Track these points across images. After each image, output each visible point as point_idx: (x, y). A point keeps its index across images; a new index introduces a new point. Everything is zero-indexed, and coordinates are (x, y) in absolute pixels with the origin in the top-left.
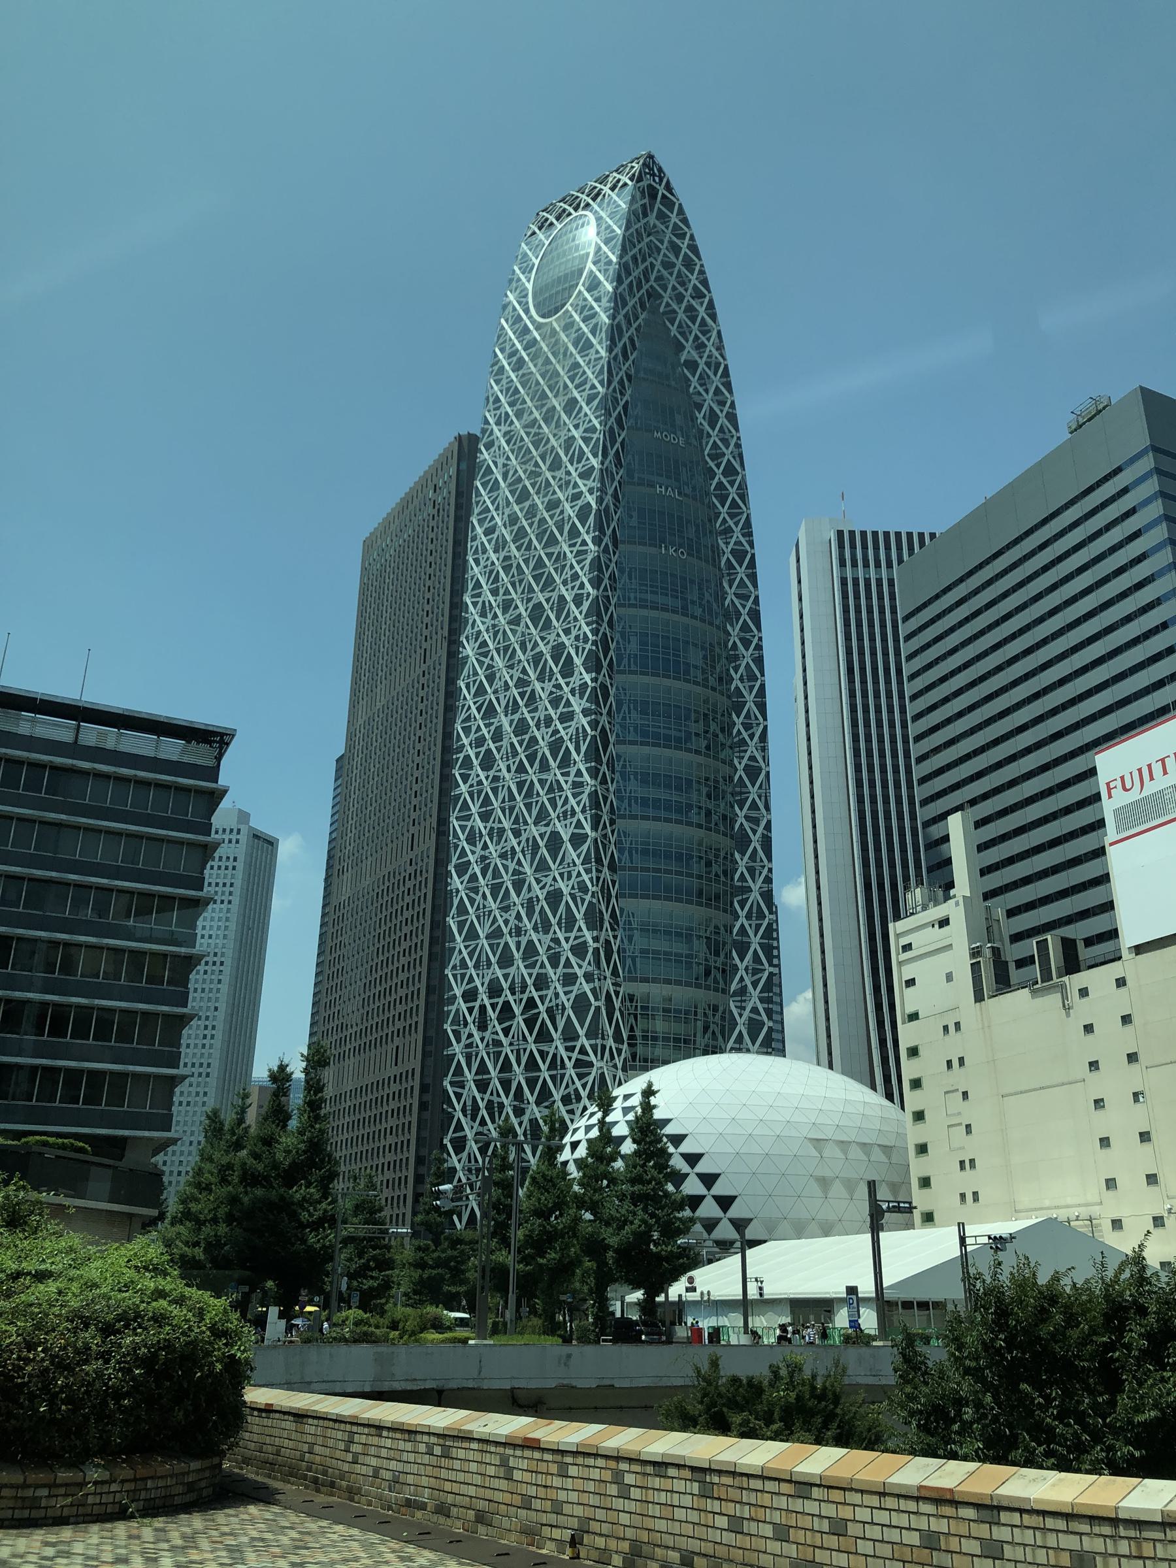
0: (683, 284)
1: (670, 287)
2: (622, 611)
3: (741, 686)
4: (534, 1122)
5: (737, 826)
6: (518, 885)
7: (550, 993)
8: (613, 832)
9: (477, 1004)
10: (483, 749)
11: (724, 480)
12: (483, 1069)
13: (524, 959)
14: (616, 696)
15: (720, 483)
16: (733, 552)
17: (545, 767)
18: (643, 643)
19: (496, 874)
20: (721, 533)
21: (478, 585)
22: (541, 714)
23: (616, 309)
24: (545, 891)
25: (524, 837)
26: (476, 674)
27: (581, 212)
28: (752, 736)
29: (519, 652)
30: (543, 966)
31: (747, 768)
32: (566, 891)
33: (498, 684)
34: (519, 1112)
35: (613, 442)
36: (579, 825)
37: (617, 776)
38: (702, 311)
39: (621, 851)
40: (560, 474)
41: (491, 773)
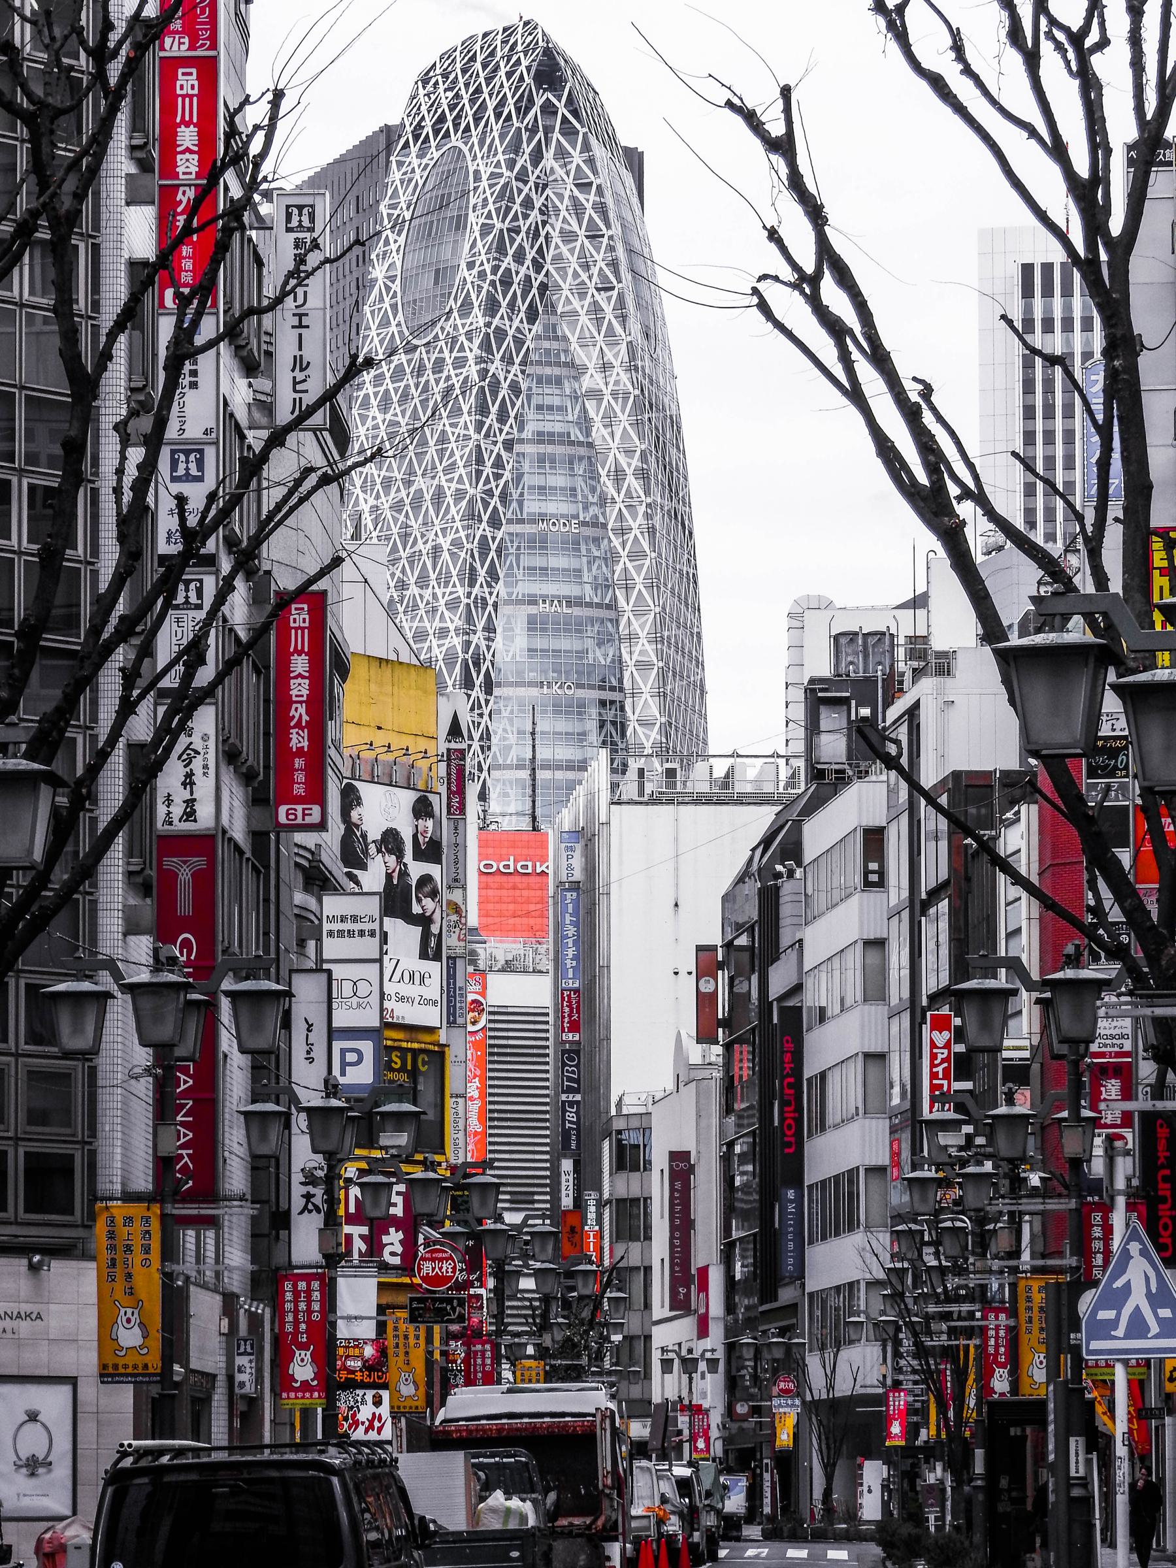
0: (586, 267)
1: (570, 272)
11: (629, 565)
38: (608, 309)
40: (427, 594)
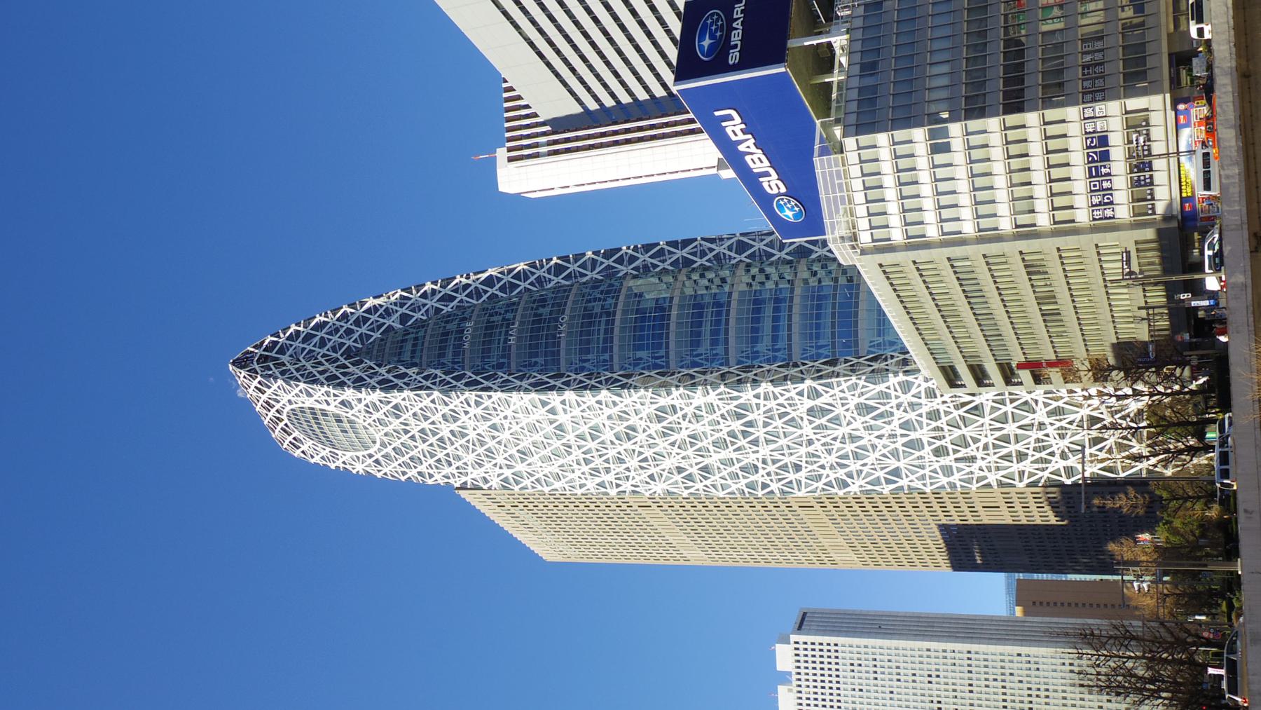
0: (337, 330)
2: (616, 367)
3: (669, 262)
4: (1050, 414)
5: (789, 258)
6: (853, 439)
7: (942, 408)
8: (804, 364)
9: (954, 465)
10: (740, 473)
11: (498, 286)
12: (1007, 457)
13: (915, 430)
14: (688, 368)
15: (501, 289)
16: (556, 275)
17: (750, 424)
18: (640, 348)
19: (846, 457)
20: (542, 286)
21: (601, 485)
22: (708, 429)
23: (367, 386)
24: (858, 417)
25: (814, 437)
26: (676, 483)
27: (284, 417)
28: (711, 250)
29: (657, 450)
30: (920, 415)
31: (739, 252)
32: (857, 400)
33: (684, 464)
34: (1041, 426)
35: (477, 383)
36: (801, 394)
37: (756, 363)
39: (819, 356)
41: (760, 465)
